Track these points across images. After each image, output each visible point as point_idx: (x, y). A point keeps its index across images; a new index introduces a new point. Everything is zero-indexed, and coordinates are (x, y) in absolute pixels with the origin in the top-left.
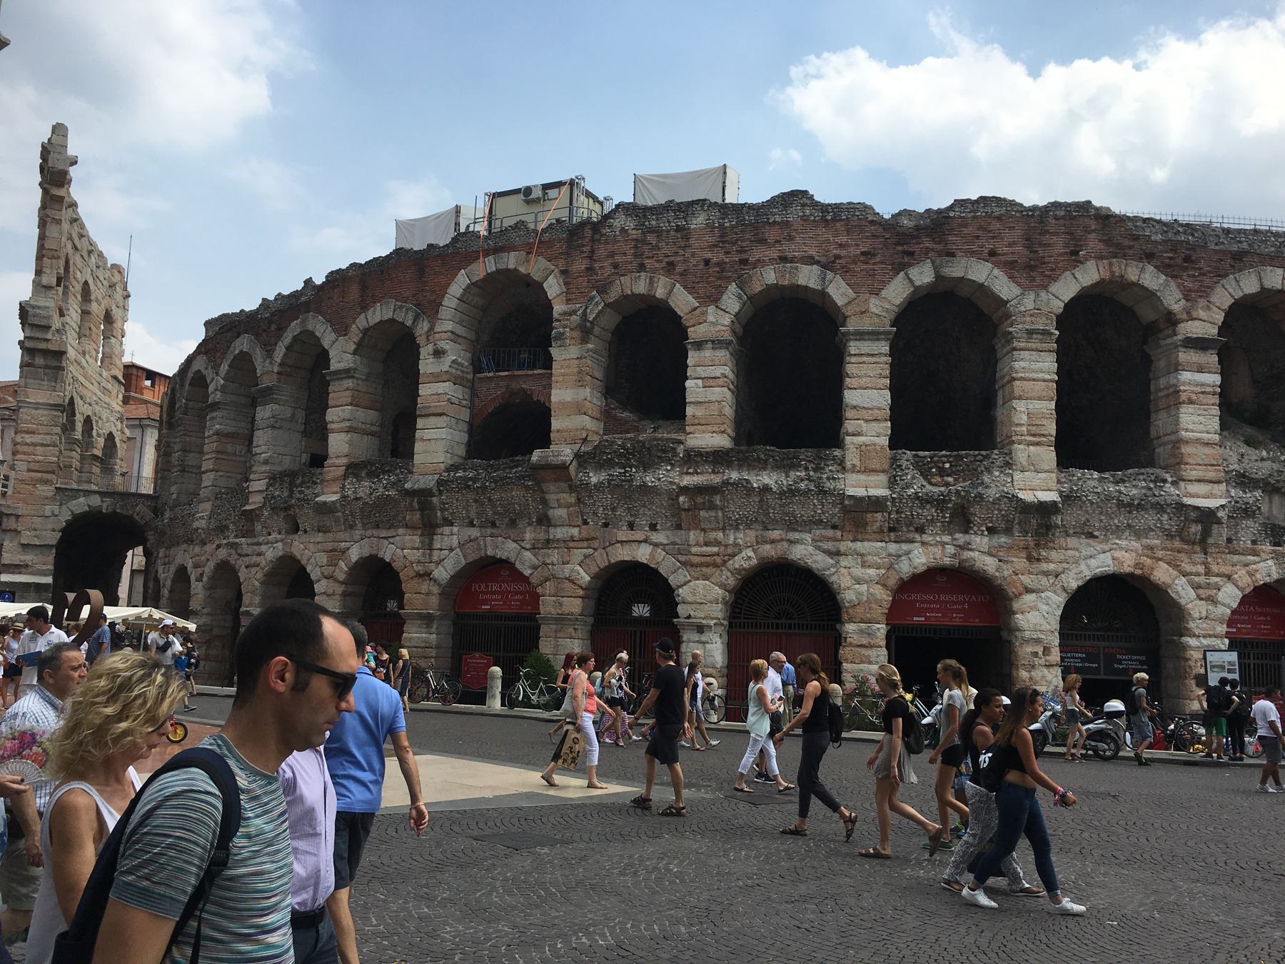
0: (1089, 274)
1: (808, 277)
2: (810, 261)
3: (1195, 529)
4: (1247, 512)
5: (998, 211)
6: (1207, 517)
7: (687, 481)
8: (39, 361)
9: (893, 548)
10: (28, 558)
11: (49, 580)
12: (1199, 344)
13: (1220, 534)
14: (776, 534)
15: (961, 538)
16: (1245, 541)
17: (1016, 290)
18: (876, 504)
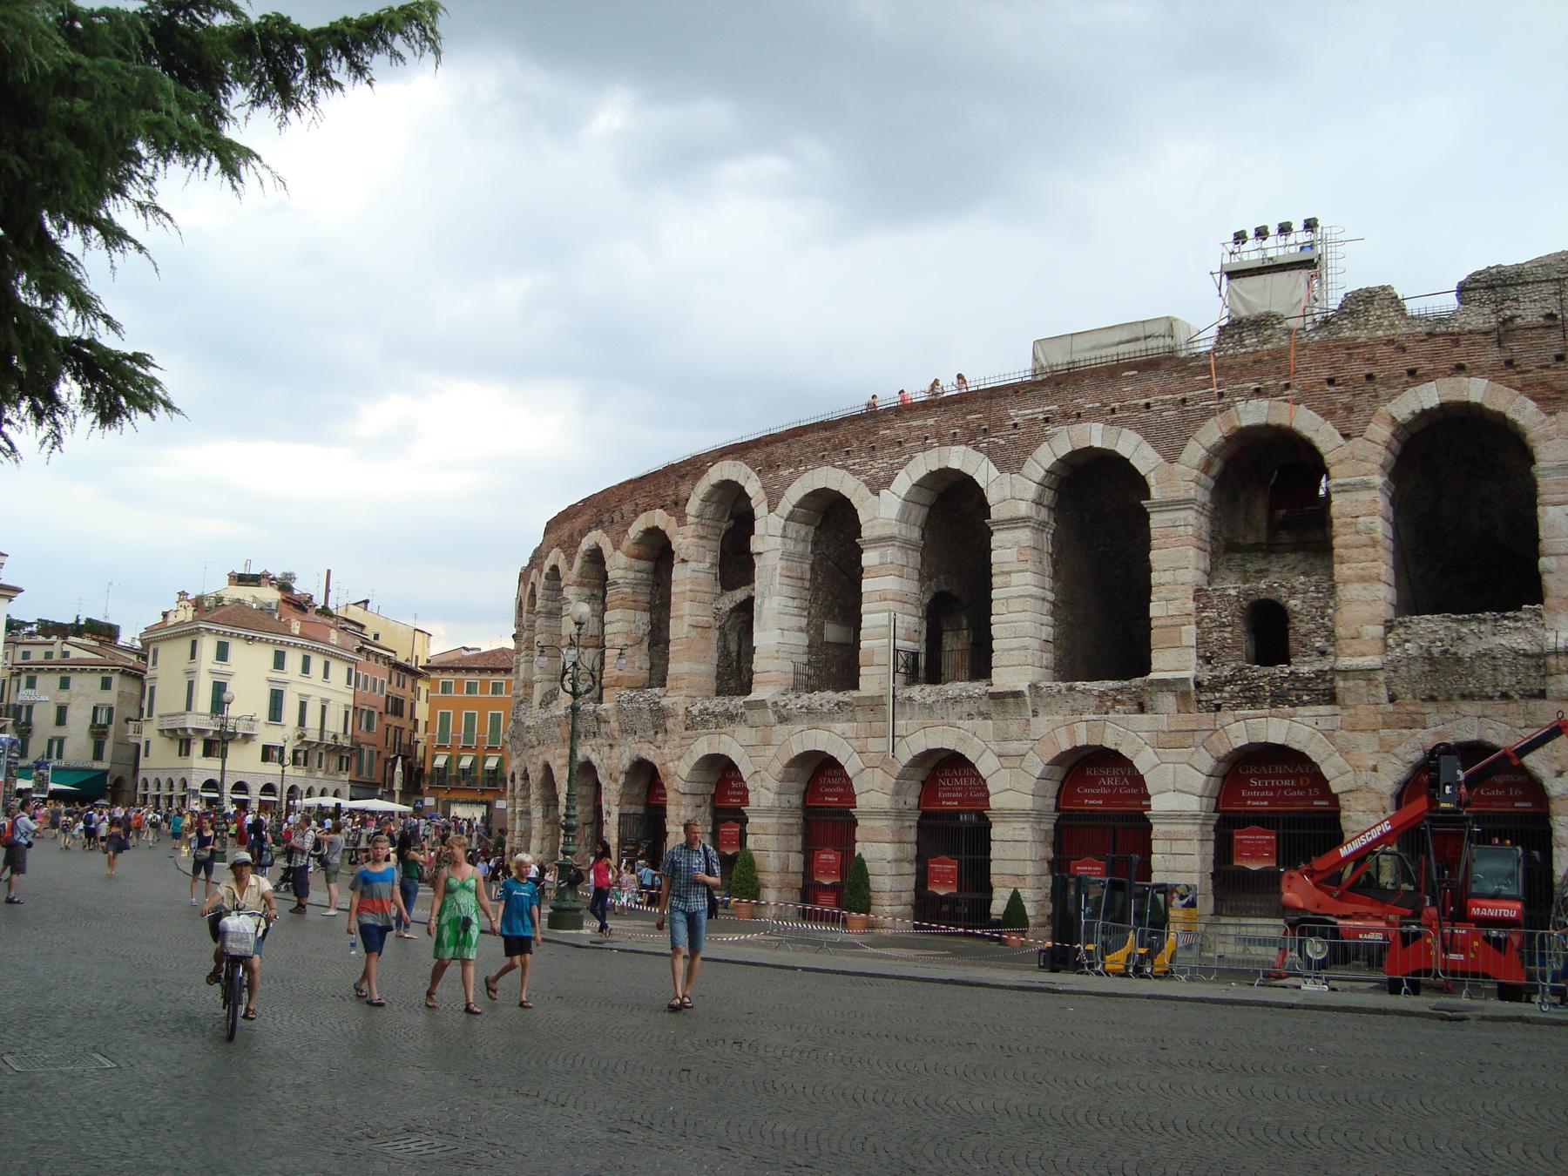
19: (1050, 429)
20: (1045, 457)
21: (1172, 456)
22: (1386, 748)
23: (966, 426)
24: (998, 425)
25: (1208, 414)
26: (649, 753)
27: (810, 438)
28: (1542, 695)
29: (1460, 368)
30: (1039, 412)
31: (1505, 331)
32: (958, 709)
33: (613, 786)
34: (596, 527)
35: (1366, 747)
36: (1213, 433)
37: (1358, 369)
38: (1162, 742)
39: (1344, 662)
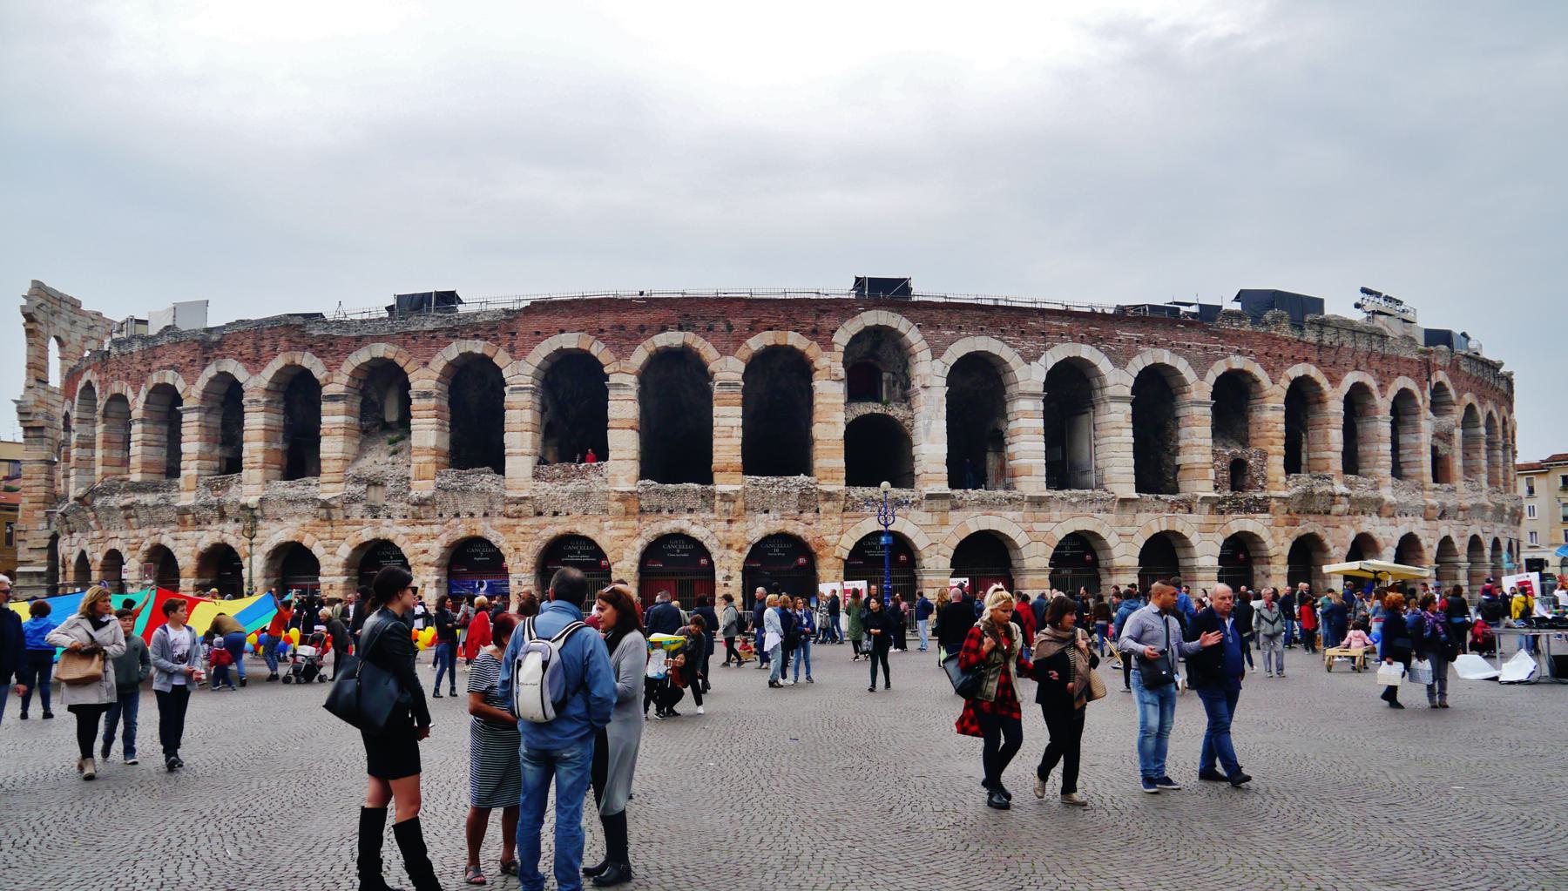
0: (278, 363)
1: (169, 377)
2: (171, 367)
3: (323, 512)
4: (353, 499)
5: (242, 328)
6: (325, 505)
7: (127, 502)
8: (30, 434)
9: (198, 534)
10: (32, 556)
11: (44, 569)
12: (333, 398)
13: (338, 515)
14: (155, 530)
15: (221, 526)
16: (356, 516)
17: (247, 375)
18: (184, 511)
19: (1141, 348)
20: (1138, 364)
21: (1201, 377)
22: (1287, 534)
23: (1089, 335)
24: (1109, 338)
25: (1218, 358)
26: (798, 529)
27: (968, 313)
28: (1328, 513)
29: (1306, 360)
30: (1135, 335)
31: (1320, 347)
32: (1093, 506)
33: (733, 554)
34: (680, 329)
35: (1281, 532)
36: (1219, 368)
37: (1276, 351)
38: (1206, 529)
39: (1273, 493)
